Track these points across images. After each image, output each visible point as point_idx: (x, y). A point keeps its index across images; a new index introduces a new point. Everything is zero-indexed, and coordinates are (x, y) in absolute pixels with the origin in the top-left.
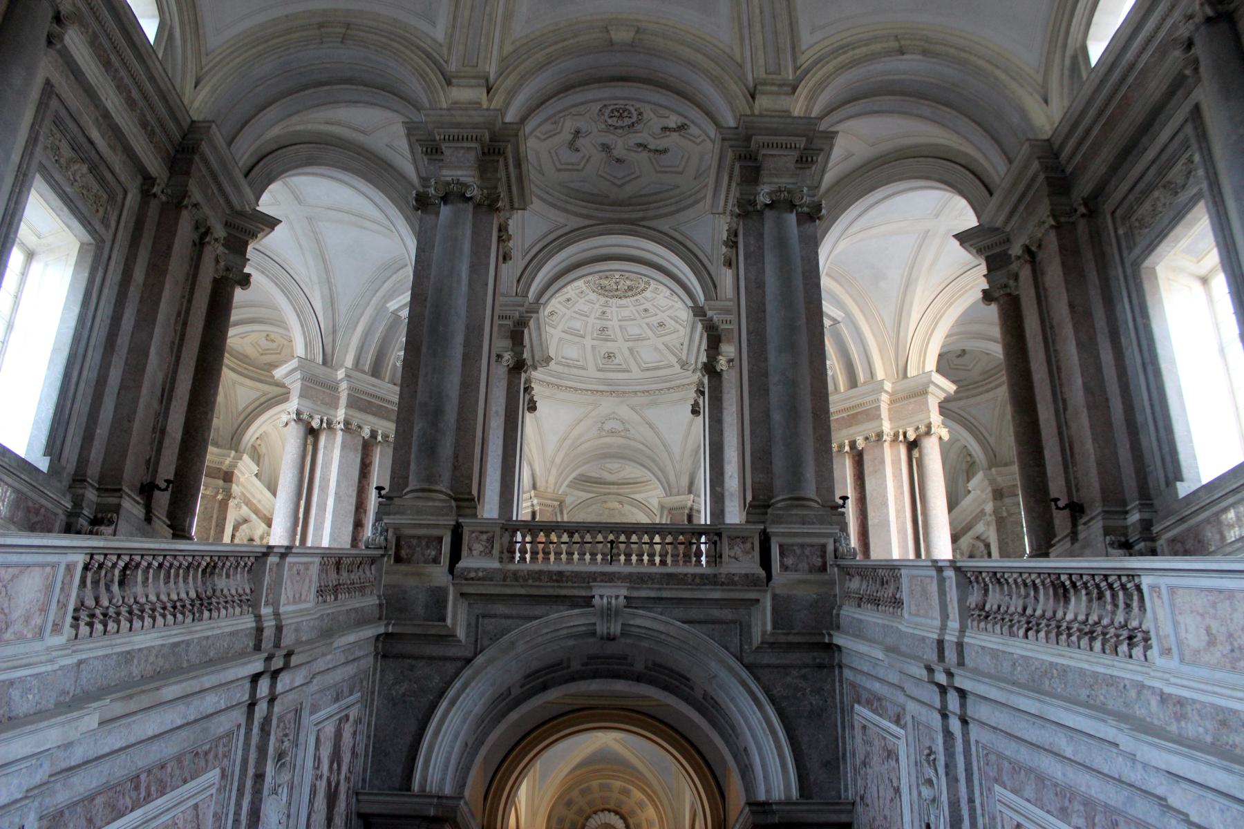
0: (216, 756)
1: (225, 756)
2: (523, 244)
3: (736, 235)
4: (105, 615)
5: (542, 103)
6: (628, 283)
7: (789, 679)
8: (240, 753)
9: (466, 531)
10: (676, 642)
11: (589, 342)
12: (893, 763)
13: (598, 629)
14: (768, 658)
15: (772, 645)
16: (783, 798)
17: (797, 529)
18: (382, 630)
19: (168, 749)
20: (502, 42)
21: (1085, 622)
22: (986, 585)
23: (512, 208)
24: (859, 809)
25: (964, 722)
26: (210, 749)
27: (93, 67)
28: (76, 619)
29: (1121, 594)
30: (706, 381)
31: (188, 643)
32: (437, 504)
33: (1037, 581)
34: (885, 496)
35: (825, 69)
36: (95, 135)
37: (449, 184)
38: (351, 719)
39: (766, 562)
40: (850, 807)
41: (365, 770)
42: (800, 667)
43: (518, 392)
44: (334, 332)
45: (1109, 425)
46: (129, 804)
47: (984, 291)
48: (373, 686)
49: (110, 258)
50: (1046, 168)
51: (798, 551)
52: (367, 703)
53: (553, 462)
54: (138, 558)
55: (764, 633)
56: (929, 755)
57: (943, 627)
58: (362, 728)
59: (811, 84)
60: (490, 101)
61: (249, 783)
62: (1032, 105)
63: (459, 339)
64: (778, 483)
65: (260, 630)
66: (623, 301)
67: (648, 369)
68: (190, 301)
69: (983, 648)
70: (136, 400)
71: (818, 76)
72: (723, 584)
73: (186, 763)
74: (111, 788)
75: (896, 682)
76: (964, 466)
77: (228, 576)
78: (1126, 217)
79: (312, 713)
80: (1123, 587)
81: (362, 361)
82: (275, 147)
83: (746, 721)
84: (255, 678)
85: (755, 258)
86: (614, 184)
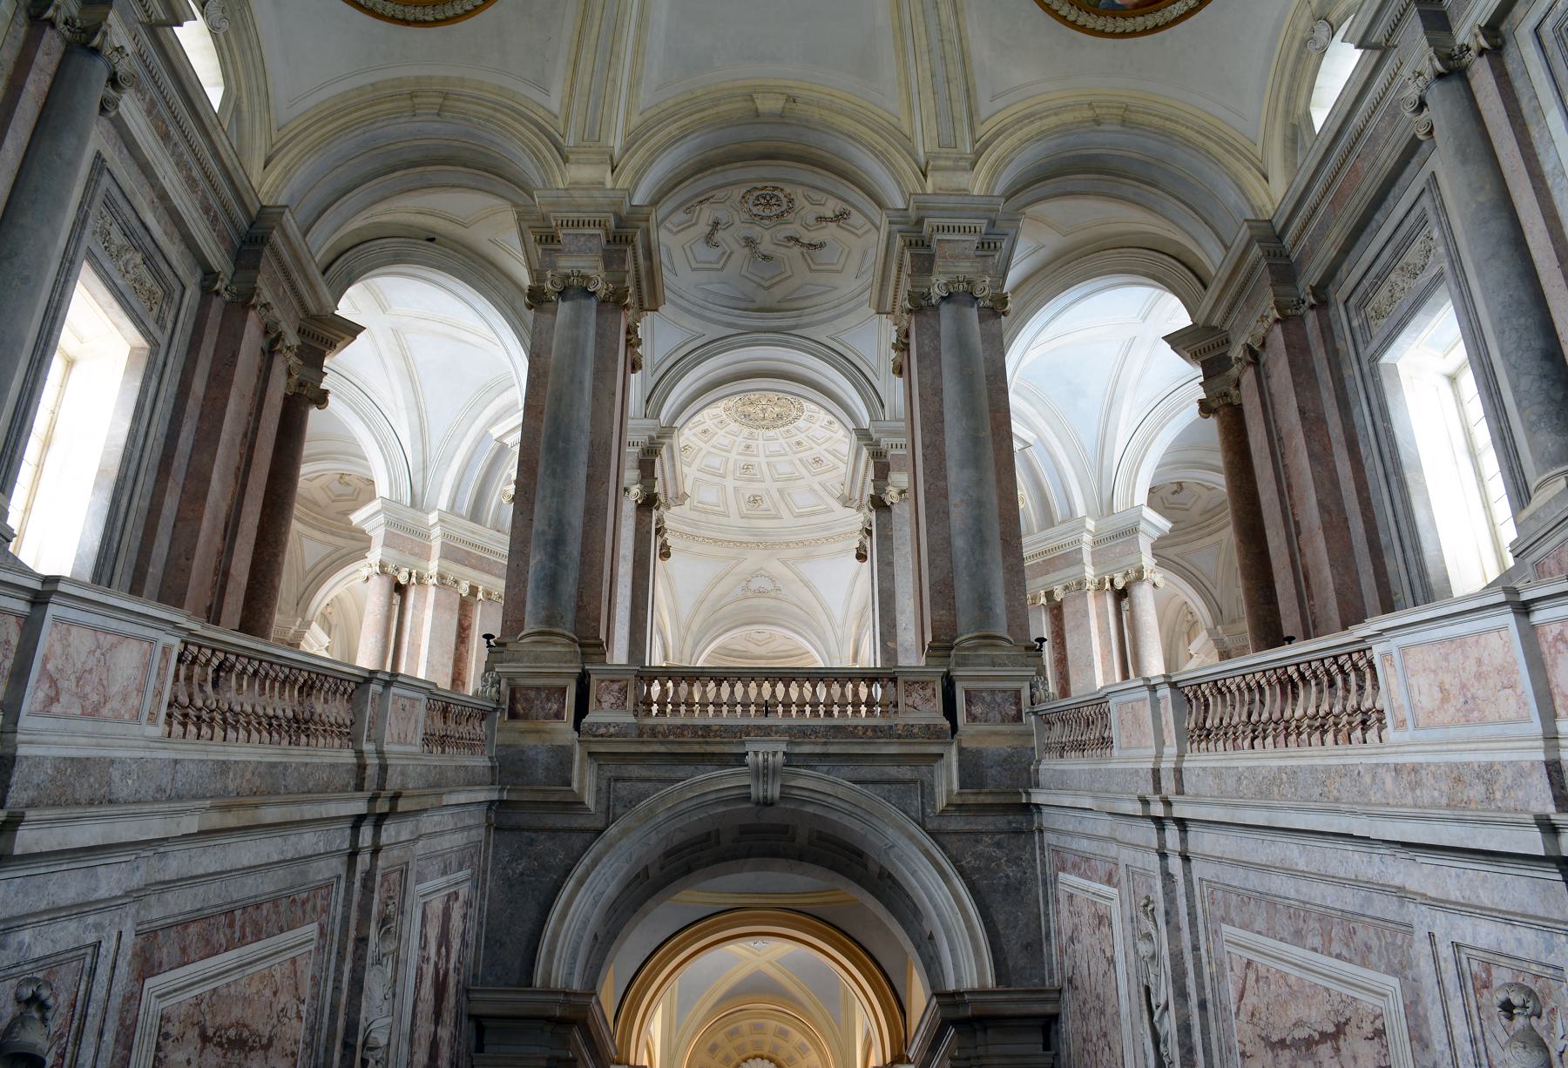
0: (314, 908)
1: (323, 911)
2: (653, 357)
3: (907, 336)
4: (199, 718)
5: (676, 185)
6: (777, 409)
7: (980, 847)
8: (340, 908)
9: (593, 678)
10: (846, 806)
11: (730, 483)
12: (1105, 930)
13: (752, 790)
14: (957, 823)
15: (960, 807)
16: (976, 986)
17: (986, 671)
18: (495, 796)
19: (264, 885)
20: (628, 113)
21: (1314, 718)
22: (1206, 700)
23: (642, 308)
24: (1067, 995)
25: (1186, 859)
26: (308, 899)
27: (150, 138)
28: (169, 715)
29: (1353, 675)
30: (873, 516)
31: (286, 766)
32: (559, 649)
33: (1263, 681)
34: (1090, 656)
35: (1008, 142)
36: (150, 220)
37: (568, 277)
38: (461, 898)
39: (950, 711)
40: (1056, 995)
41: (476, 964)
42: (993, 833)
43: (649, 532)
44: (425, 468)
45: (1349, 548)
46: (224, 941)
47: (1201, 402)
48: (485, 864)
49: (165, 364)
50: (1268, 255)
51: (988, 699)
52: (478, 882)
53: (688, 628)
54: (233, 658)
55: (950, 792)
56: (1146, 906)
57: (1159, 756)
58: (472, 912)
59: (992, 159)
60: (615, 181)
61: (350, 946)
62: (1251, 179)
63: (583, 457)
64: (963, 621)
65: (361, 767)
66: (771, 433)
67: (801, 515)
68: (258, 419)
69: (1204, 769)
70: (195, 534)
71: (1000, 150)
72: (899, 736)
73: (282, 909)
74: (199, 917)
75: (1106, 833)
76: (1185, 627)
77: (326, 701)
78: (1362, 305)
79: (418, 882)
80: (1355, 667)
81: (458, 504)
82: (357, 241)
83: (931, 899)
84: (358, 821)
85: (930, 360)
86: (760, 285)
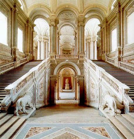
39: (79, 58)
45: (108, 45)
62: (106, 13)
